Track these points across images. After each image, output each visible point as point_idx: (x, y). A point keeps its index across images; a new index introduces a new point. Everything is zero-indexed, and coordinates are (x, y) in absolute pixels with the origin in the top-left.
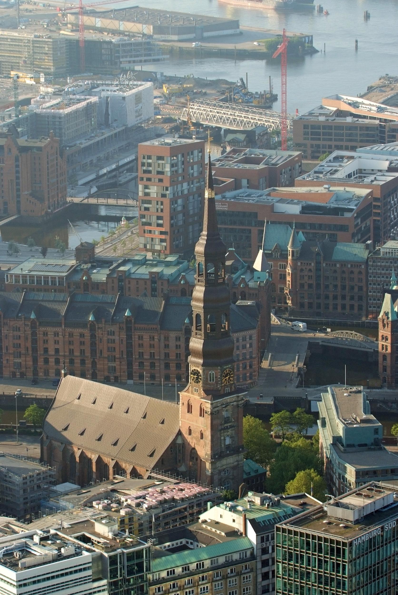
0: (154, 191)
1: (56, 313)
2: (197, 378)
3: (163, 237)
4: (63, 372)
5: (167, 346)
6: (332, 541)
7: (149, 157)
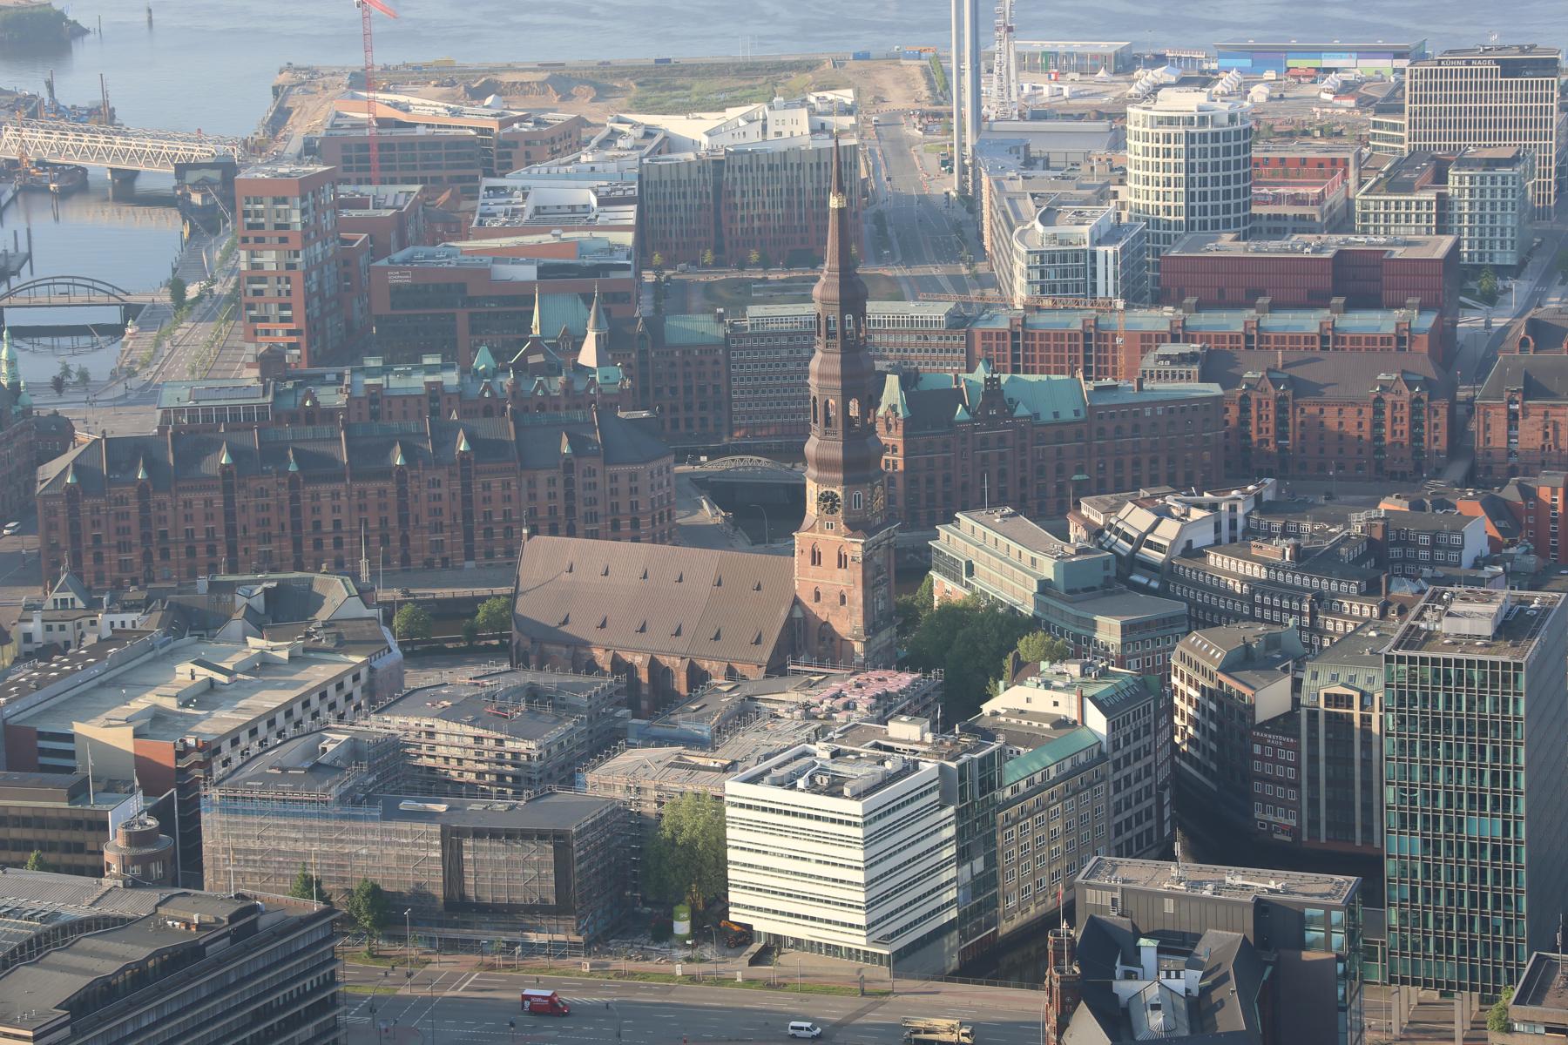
1: (332, 461)
2: (832, 506)
3: (294, 339)
4: (525, 531)
5: (532, 497)
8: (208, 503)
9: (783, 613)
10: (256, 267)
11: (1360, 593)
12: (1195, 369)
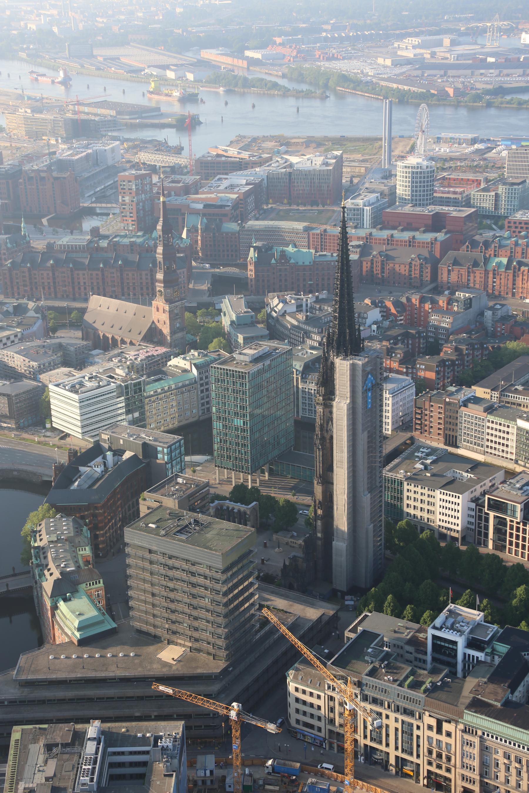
0: (127, 199)
5: (141, 279)
6: (239, 372)
7: (124, 181)
8: (48, 274)
9: (149, 326)
10: (124, 201)
11: (318, 333)
12: (358, 250)
